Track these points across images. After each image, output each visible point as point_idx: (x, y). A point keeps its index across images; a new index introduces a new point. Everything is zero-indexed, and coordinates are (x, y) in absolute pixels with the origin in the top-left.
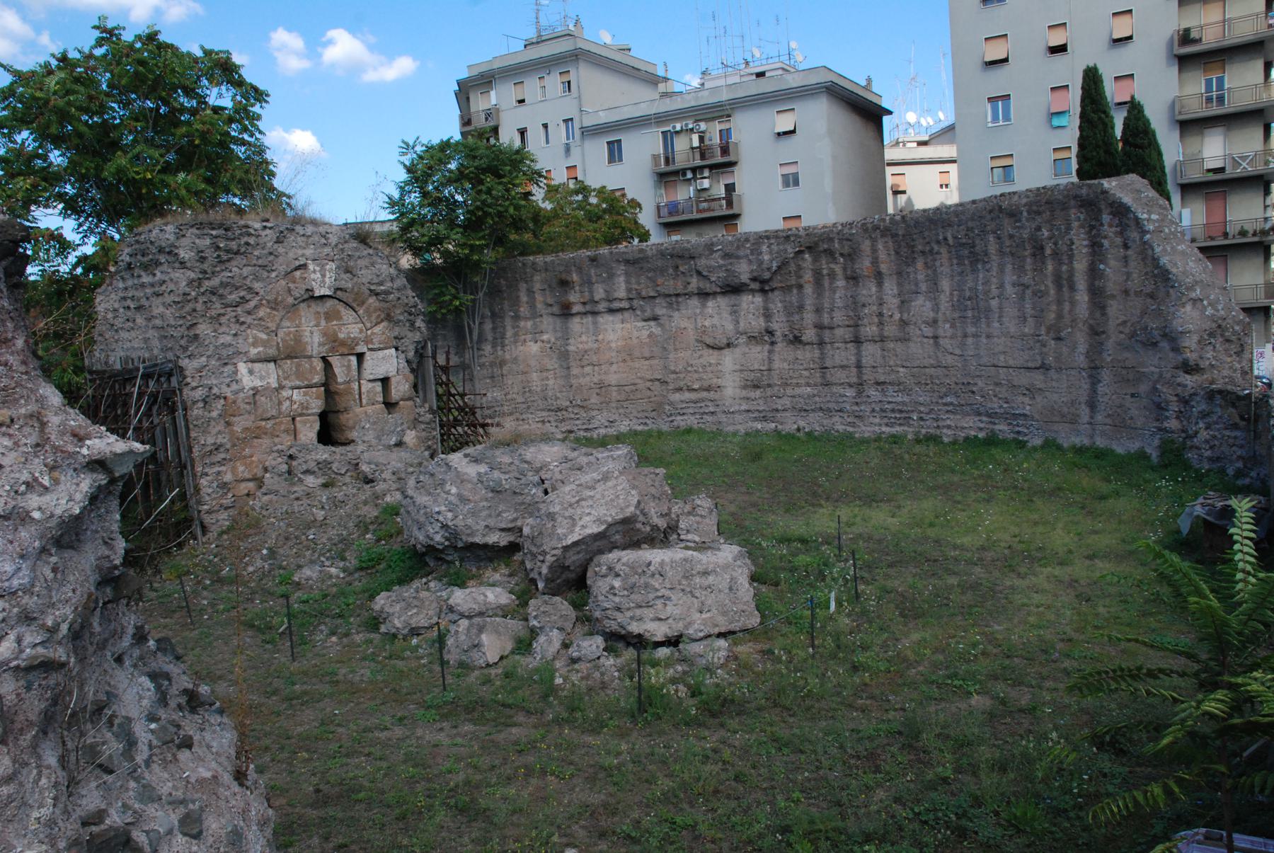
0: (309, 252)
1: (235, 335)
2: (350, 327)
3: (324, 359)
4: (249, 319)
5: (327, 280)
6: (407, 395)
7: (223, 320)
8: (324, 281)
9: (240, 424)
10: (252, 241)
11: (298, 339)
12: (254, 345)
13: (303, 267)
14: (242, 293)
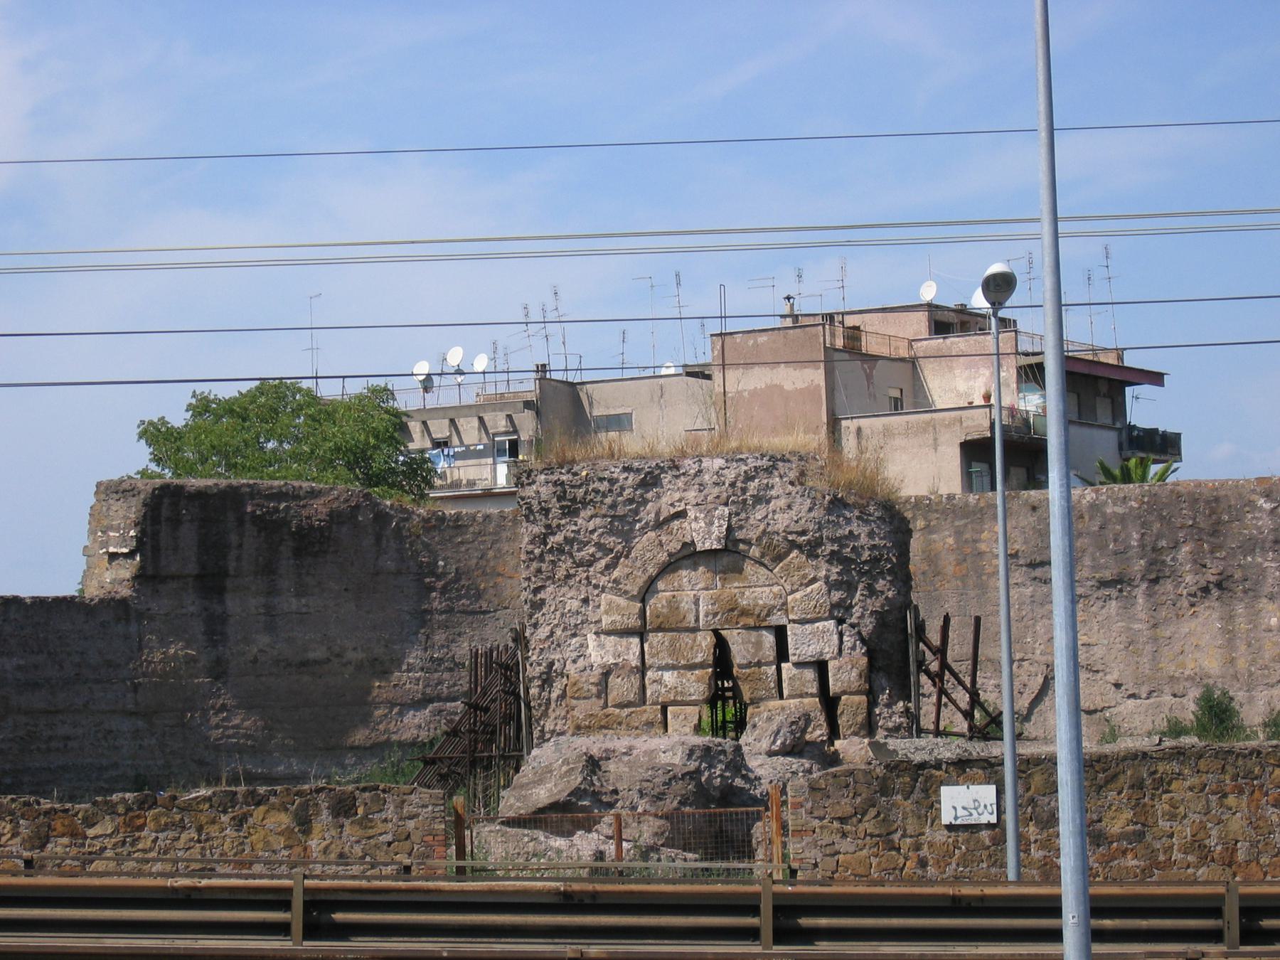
0: (691, 495)
1: (585, 601)
2: (758, 588)
3: (716, 632)
4: (603, 580)
5: (715, 529)
6: (855, 686)
7: (571, 582)
8: (710, 533)
9: (582, 710)
10: (604, 486)
11: (673, 605)
12: (606, 612)
13: (681, 515)
14: (592, 550)
